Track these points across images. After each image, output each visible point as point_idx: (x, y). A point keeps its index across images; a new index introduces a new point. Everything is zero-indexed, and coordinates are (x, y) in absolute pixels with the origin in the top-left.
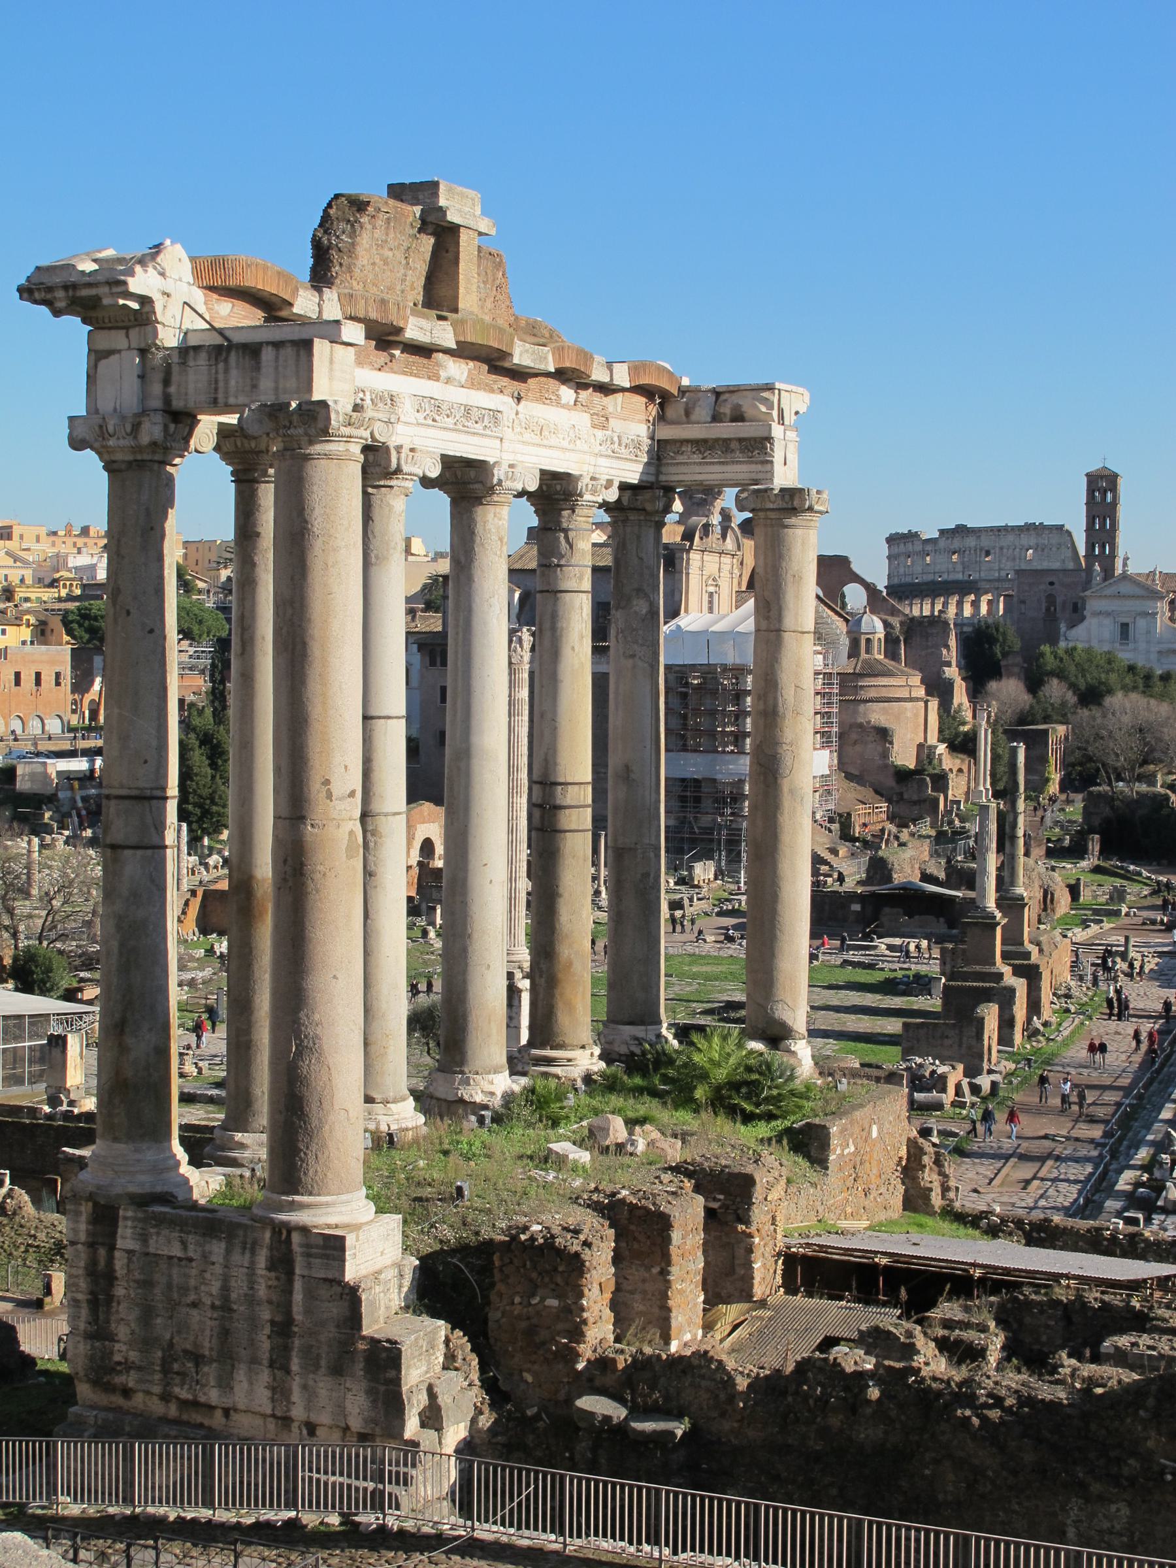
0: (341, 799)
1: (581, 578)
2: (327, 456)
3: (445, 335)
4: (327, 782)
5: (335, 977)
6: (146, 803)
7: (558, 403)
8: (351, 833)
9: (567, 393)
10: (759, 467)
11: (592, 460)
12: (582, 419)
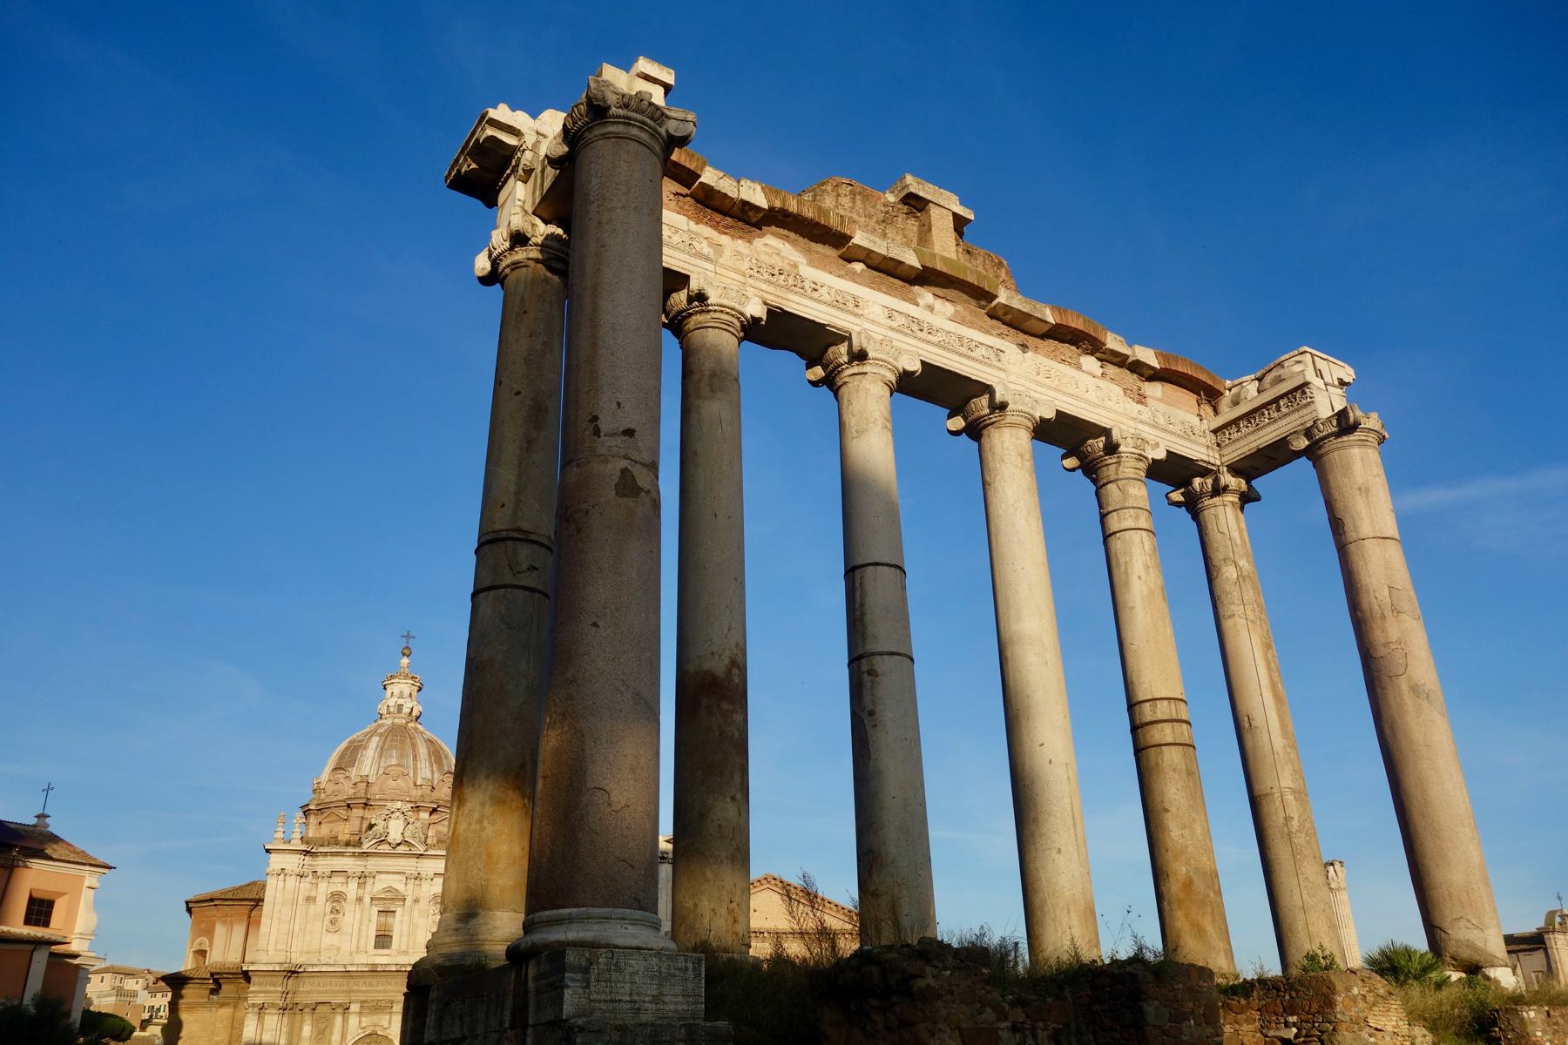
0: (611, 435)
1: (1137, 518)
2: (605, 136)
3: (912, 260)
4: (595, 419)
5: (595, 625)
6: (501, 545)
7: (1079, 368)
8: (625, 471)
9: (1090, 363)
10: (1305, 411)
11: (1133, 424)
12: (1119, 390)
